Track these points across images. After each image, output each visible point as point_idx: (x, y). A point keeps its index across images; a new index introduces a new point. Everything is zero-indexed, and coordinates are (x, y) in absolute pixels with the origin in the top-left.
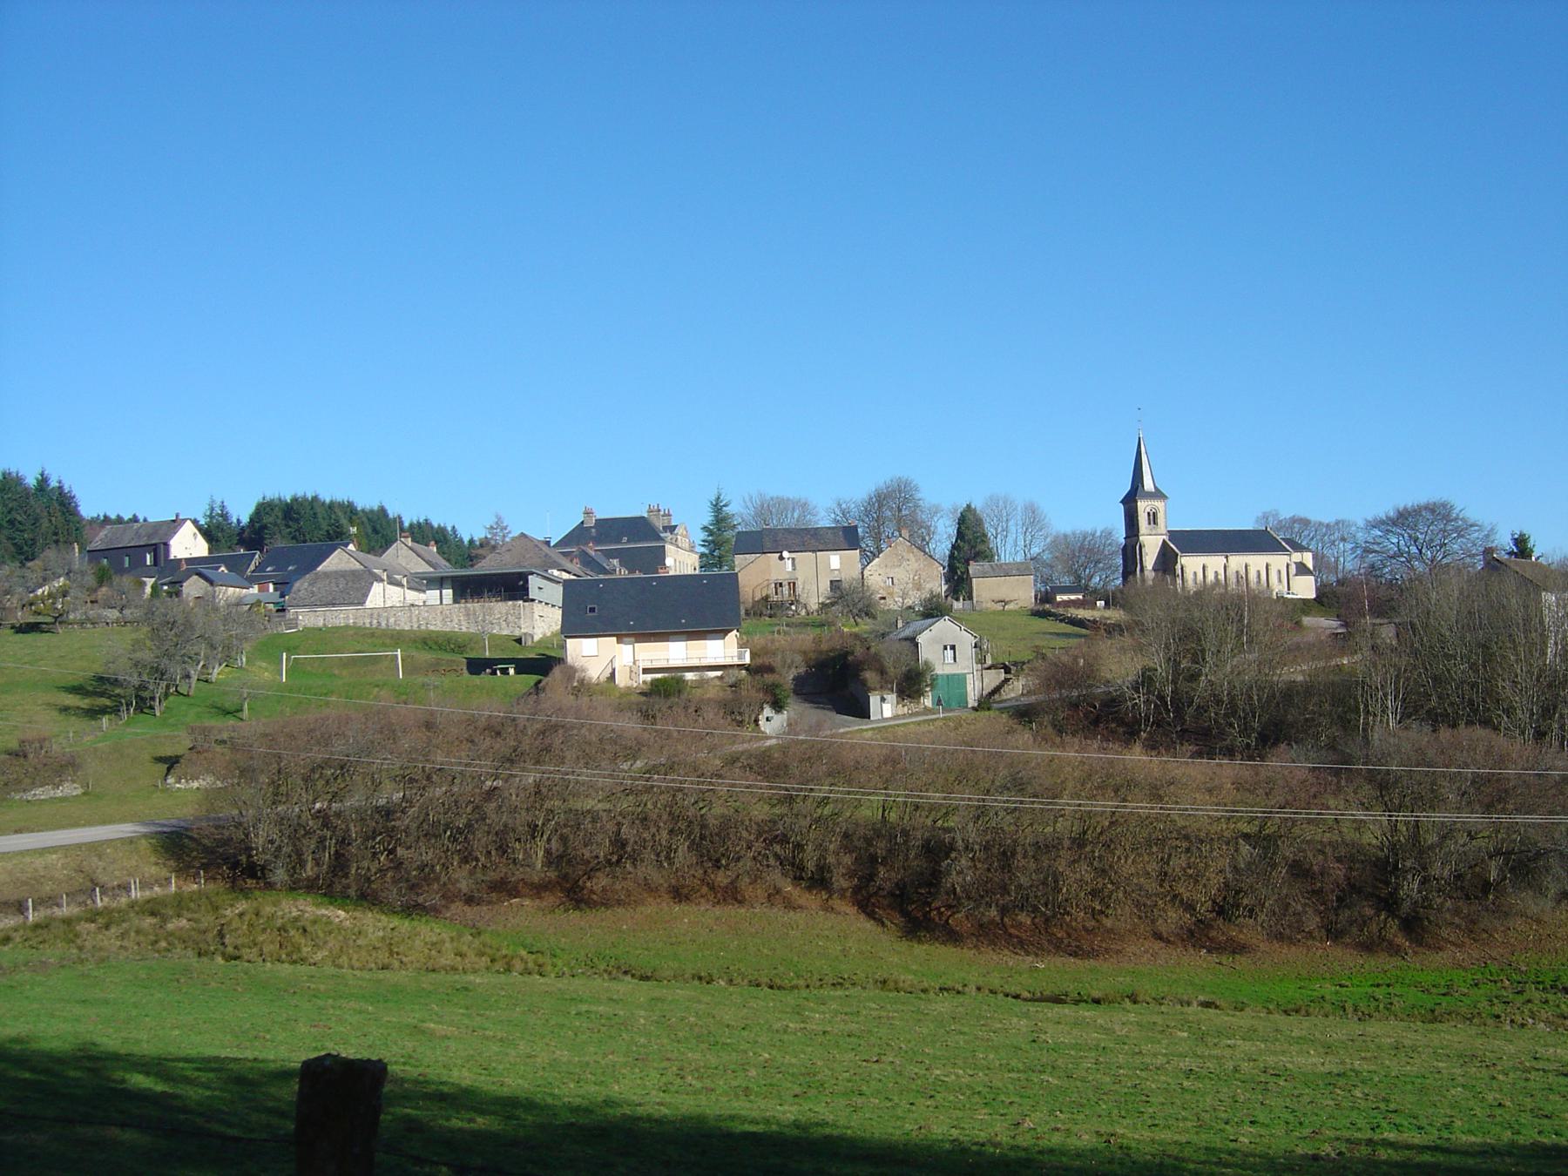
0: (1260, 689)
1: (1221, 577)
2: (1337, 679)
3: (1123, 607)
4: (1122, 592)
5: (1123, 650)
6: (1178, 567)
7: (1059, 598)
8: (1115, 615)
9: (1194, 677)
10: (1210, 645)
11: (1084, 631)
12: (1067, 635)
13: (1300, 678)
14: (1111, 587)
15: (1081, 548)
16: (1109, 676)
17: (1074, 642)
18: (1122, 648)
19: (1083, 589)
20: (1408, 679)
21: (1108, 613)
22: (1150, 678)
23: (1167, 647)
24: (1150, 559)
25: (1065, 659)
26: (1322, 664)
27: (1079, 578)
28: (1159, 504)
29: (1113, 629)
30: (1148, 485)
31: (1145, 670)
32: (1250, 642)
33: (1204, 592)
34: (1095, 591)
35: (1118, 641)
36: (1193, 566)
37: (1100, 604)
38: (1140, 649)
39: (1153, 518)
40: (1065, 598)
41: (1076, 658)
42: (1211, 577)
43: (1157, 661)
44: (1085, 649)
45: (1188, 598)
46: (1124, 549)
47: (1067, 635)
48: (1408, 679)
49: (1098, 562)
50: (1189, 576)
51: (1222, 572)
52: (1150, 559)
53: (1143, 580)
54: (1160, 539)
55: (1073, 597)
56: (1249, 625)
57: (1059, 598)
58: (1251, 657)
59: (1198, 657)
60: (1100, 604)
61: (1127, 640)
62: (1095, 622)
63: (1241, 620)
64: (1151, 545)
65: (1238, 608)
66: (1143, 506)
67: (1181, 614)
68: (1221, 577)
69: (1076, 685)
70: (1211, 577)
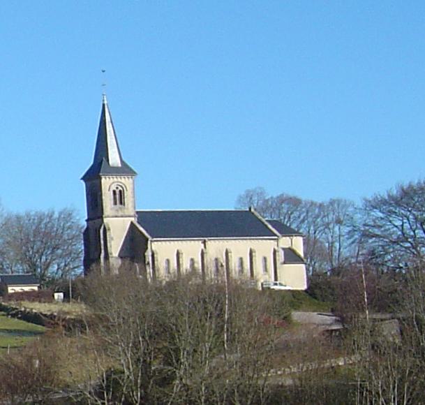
0: (243, 394)
1: (198, 265)
2: (331, 383)
3: (84, 300)
4: (83, 282)
5: (85, 349)
6: (148, 254)
7: (11, 290)
8: (76, 309)
9: (166, 381)
10: (185, 344)
11: (40, 328)
12: (20, 333)
13: (289, 382)
14: (71, 277)
15: (37, 232)
16: (68, 380)
17: (27, 340)
18: (84, 347)
19: (40, 280)
20: (413, 383)
21: (67, 307)
22: (116, 382)
23: (136, 345)
24: (115, 245)
25: (18, 359)
26: (314, 365)
27: (34, 266)
28: (126, 182)
29: (73, 326)
30: (114, 159)
31: (110, 373)
32: (231, 340)
33: (177, 284)
34: (53, 281)
35: (79, 339)
36: (167, 253)
37: (59, 296)
38: (104, 348)
39: (119, 197)
40: (18, 289)
41: (30, 359)
42: (186, 265)
43: (125, 362)
44: (41, 349)
45: (159, 289)
46: (86, 233)
47: (20, 333)
48: (413, 383)
49: (56, 248)
50: (161, 264)
51: (198, 259)
52: (115, 245)
53: (108, 269)
54: (127, 222)
55: (27, 289)
56: (230, 321)
57: (11, 290)
58: (232, 358)
59: (171, 357)
60: (59, 296)
61: (89, 338)
62: (52, 317)
63: (221, 315)
64: (117, 228)
65: (217, 299)
66: (108, 184)
67: (152, 308)
68: (198, 265)
69: (30, 390)
70: (186, 265)
